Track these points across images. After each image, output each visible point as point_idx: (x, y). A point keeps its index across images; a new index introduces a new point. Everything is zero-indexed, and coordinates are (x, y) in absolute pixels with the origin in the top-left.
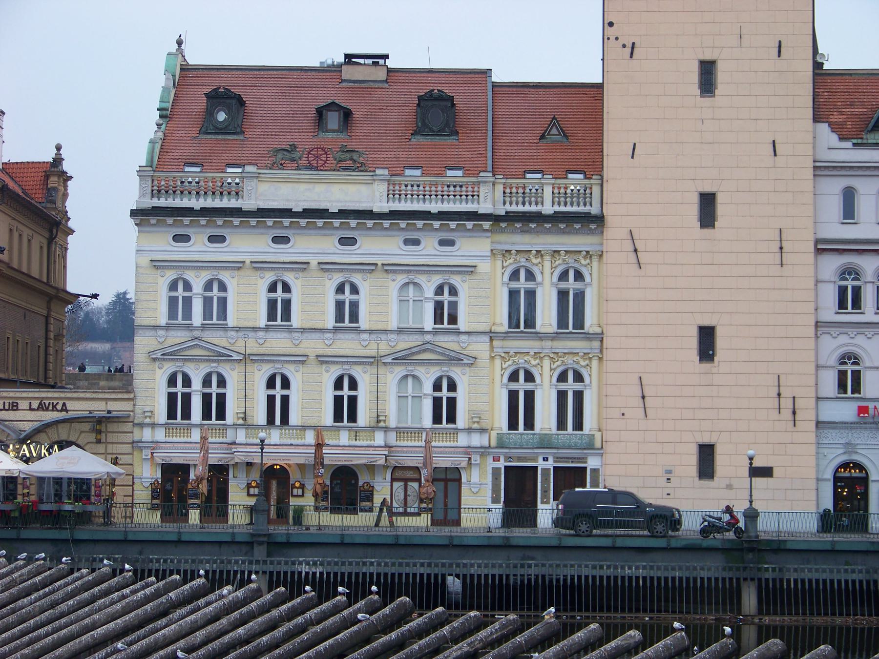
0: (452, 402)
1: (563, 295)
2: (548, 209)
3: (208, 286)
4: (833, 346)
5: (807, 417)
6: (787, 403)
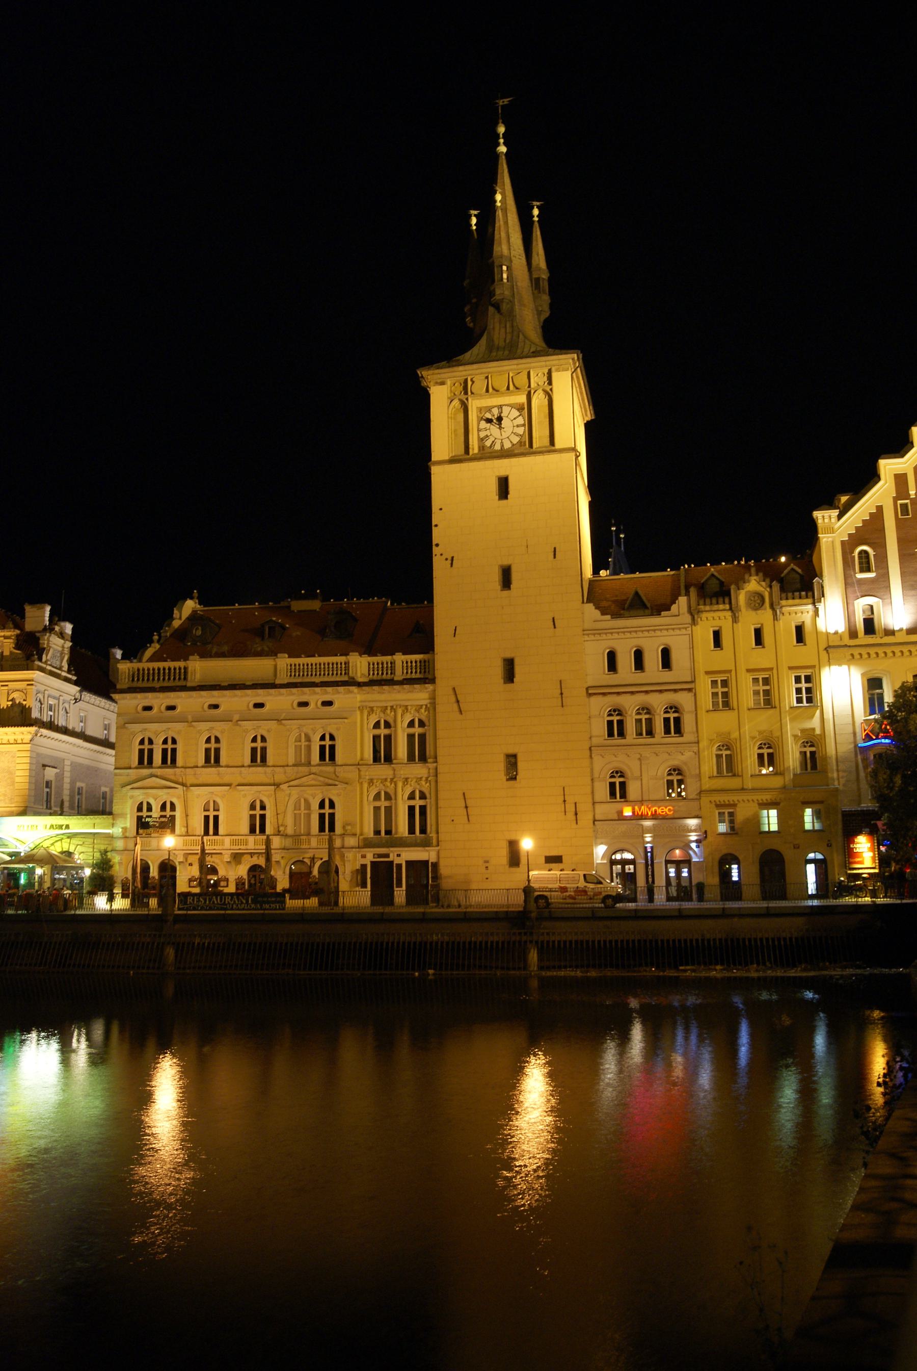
0: (332, 816)
1: (411, 737)
2: (399, 676)
3: (165, 742)
4: (604, 764)
5: (586, 818)
6: (571, 808)
